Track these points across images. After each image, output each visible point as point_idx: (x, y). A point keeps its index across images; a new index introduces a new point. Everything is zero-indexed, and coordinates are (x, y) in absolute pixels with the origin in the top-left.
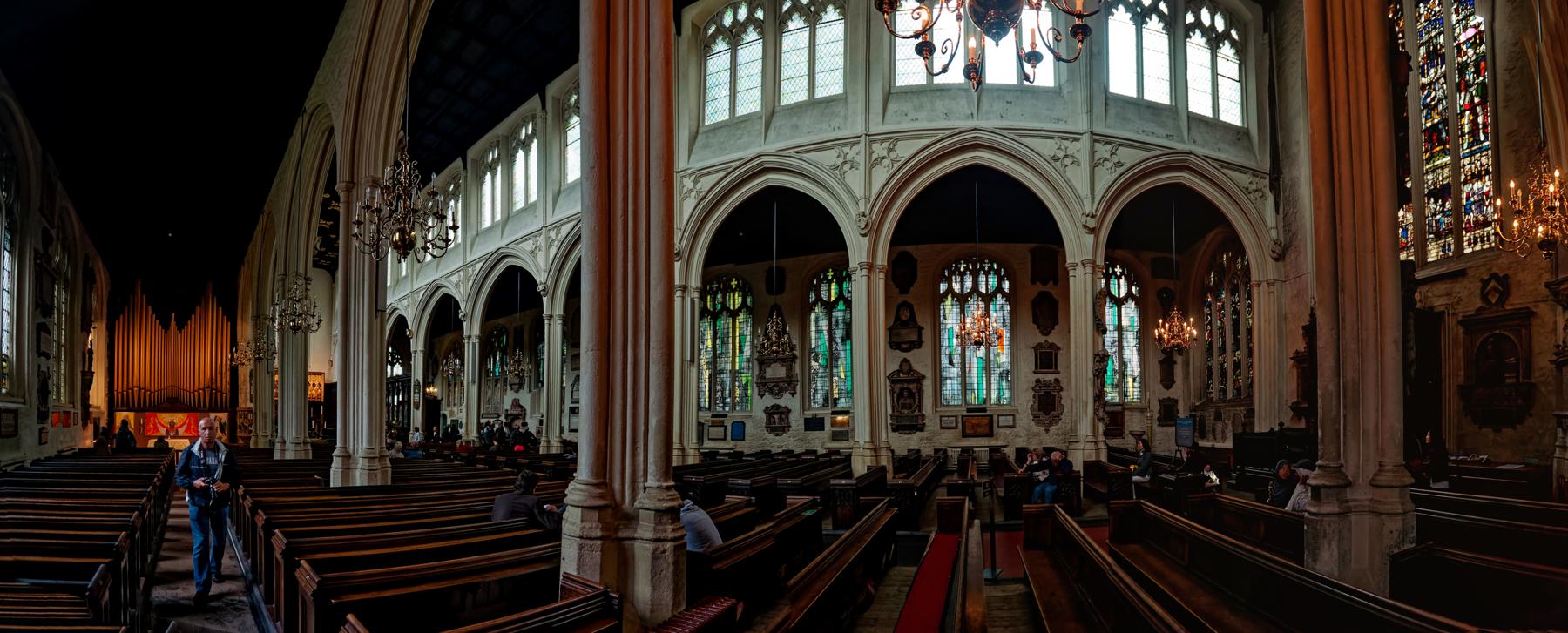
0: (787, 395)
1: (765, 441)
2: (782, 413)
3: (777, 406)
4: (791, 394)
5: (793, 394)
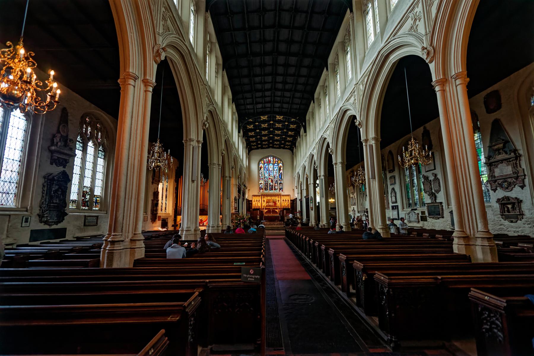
0: (517, 189)
1: (502, 227)
2: (513, 204)
3: (508, 198)
4: (520, 186)
5: (522, 187)
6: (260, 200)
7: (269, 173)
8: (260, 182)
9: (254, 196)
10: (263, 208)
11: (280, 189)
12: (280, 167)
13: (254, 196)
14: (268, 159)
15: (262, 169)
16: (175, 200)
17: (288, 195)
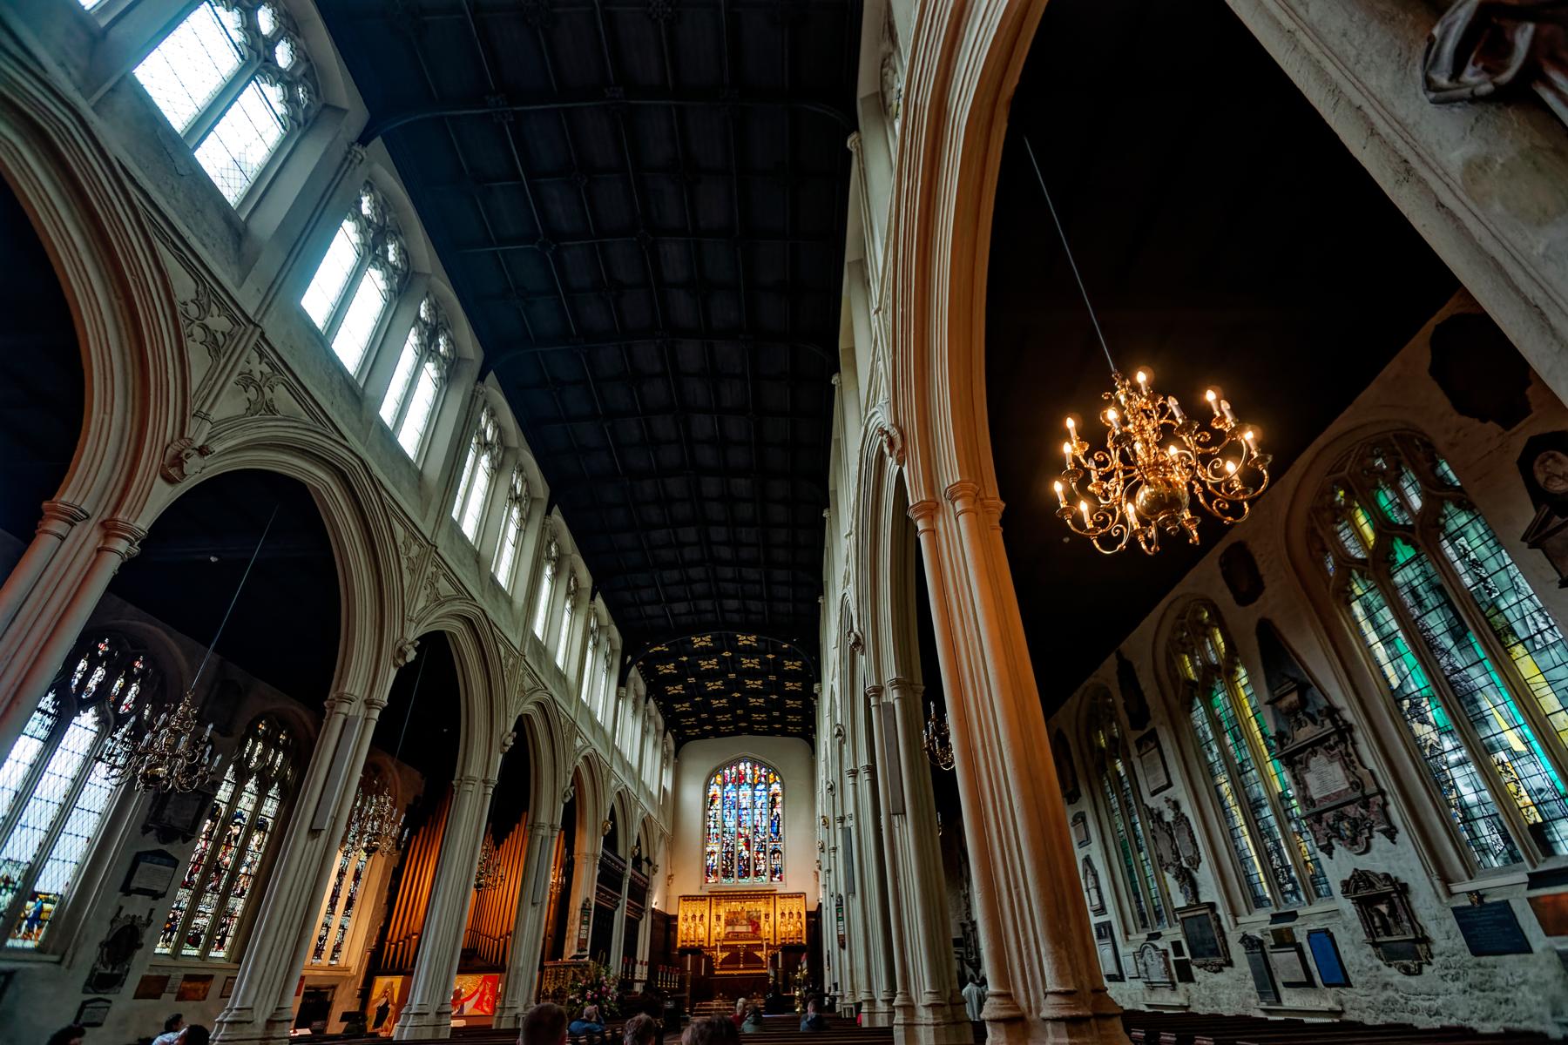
6: (707, 914)
7: (740, 816)
8: (709, 849)
9: (686, 898)
10: (712, 944)
11: (774, 873)
12: (775, 795)
13: (686, 898)
14: (738, 769)
15: (718, 802)
16: (382, 914)
17: (799, 895)
